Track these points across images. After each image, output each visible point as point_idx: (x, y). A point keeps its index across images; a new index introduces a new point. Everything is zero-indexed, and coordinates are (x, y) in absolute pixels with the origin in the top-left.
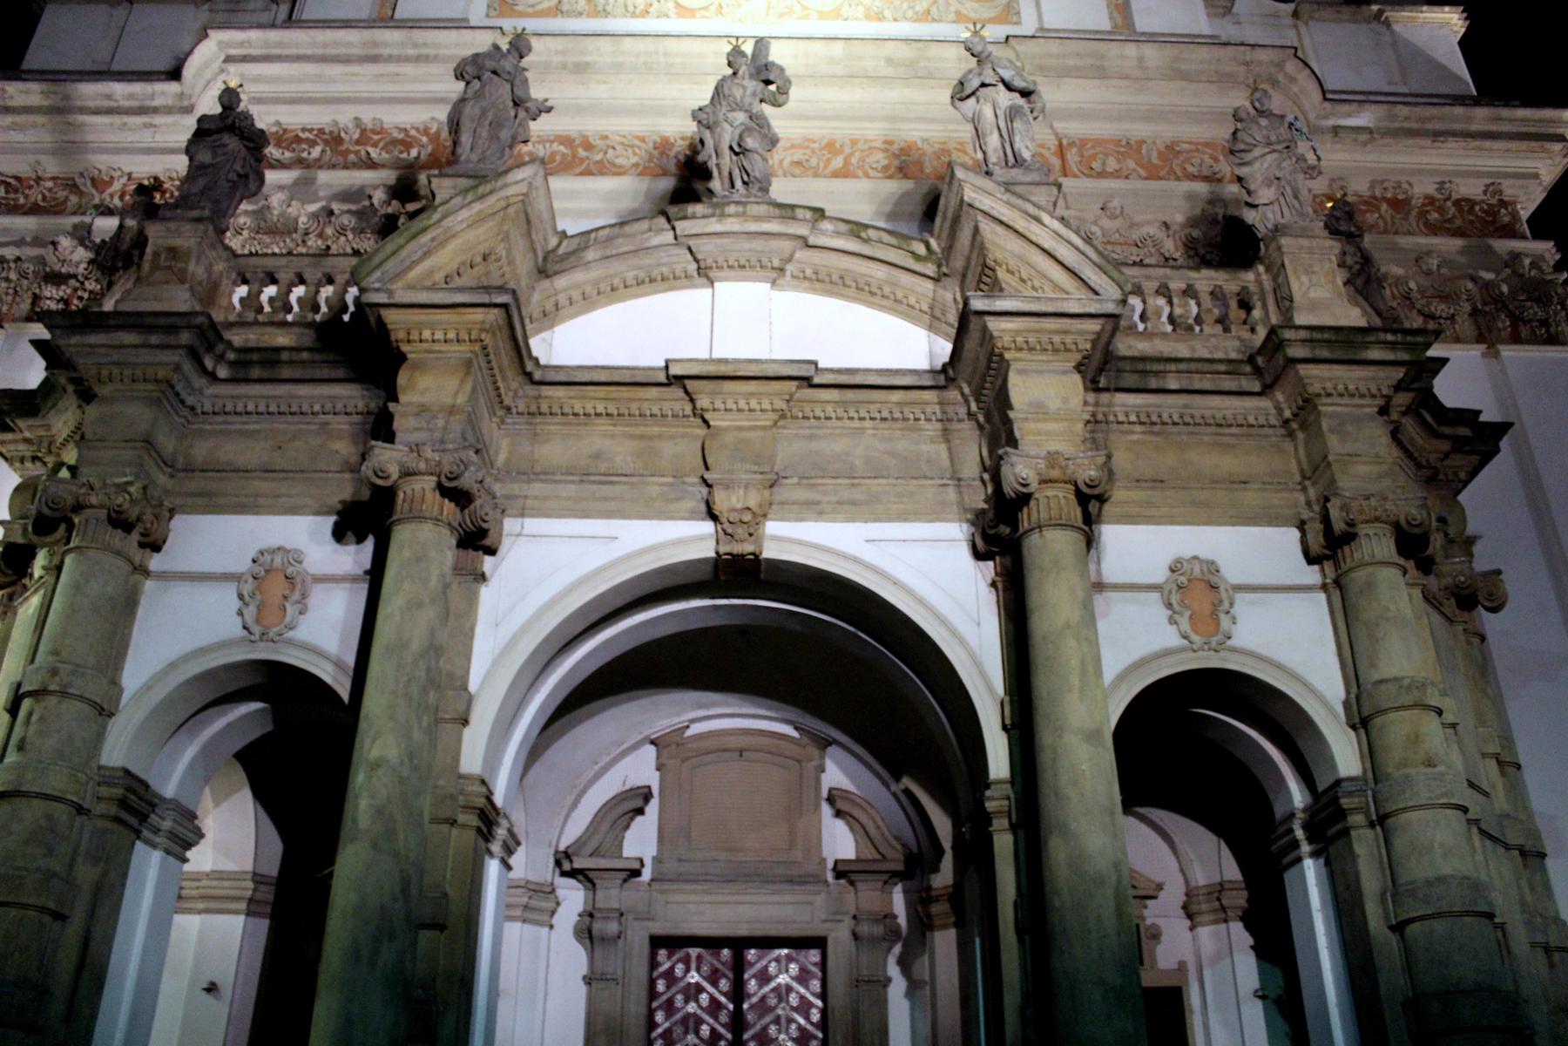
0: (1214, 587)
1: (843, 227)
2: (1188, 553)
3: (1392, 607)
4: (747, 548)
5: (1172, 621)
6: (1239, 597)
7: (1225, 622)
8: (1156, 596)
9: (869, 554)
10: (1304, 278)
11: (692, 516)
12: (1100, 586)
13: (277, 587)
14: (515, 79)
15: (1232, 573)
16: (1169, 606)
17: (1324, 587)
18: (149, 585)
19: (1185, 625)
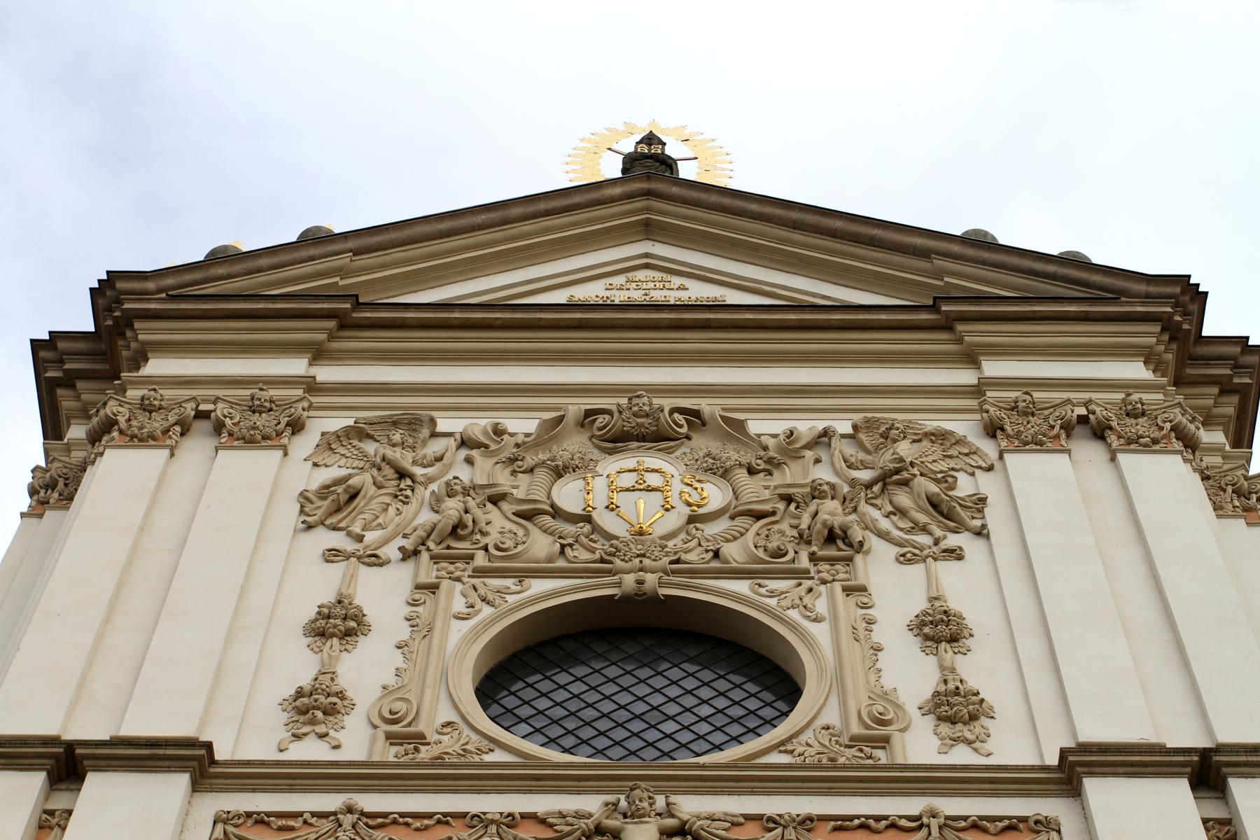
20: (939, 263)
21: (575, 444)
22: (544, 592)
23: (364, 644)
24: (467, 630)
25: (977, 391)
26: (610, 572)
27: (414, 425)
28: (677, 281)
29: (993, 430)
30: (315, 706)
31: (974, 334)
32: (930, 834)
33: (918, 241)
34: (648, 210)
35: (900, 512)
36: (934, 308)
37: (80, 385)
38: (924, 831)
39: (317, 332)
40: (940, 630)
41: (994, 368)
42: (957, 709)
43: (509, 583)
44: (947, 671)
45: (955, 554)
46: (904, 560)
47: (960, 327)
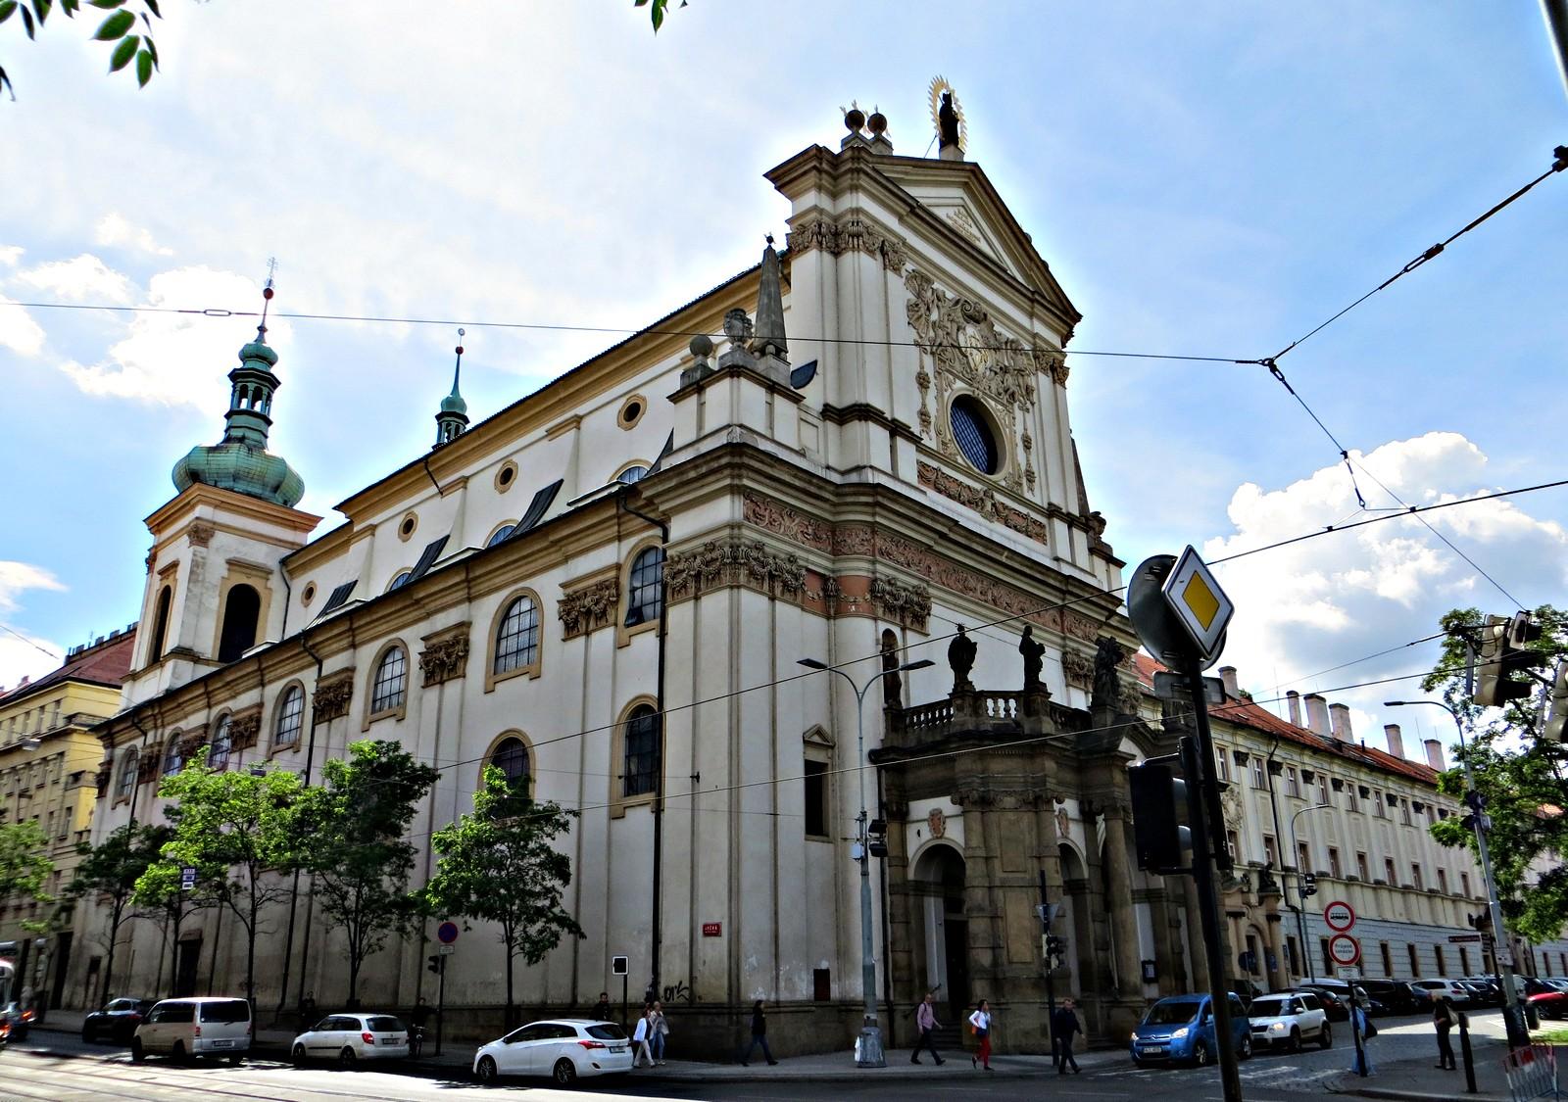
20: (1033, 265)
21: (958, 314)
22: (960, 387)
23: (929, 391)
24: (949, 396)
25: (1035, 335)
26: (971, 385)
27: (929, 281)
28: (970, 222)
29: (1036, 357)
30: (924, 415)
31: (1038, 309)
33: (1032, 254)
34: (969, 178)
35: (1019, 386)
36: (1033, 293)
37: (824, 176)
39: (903, 209)
40: (1027, 443)
41: (1039, 328)
42: (1030, 476)
43: (951, 377)
44: (1028, 464)
45: (1028, 410)
46: (1020, 408)
47: (1036, 305)
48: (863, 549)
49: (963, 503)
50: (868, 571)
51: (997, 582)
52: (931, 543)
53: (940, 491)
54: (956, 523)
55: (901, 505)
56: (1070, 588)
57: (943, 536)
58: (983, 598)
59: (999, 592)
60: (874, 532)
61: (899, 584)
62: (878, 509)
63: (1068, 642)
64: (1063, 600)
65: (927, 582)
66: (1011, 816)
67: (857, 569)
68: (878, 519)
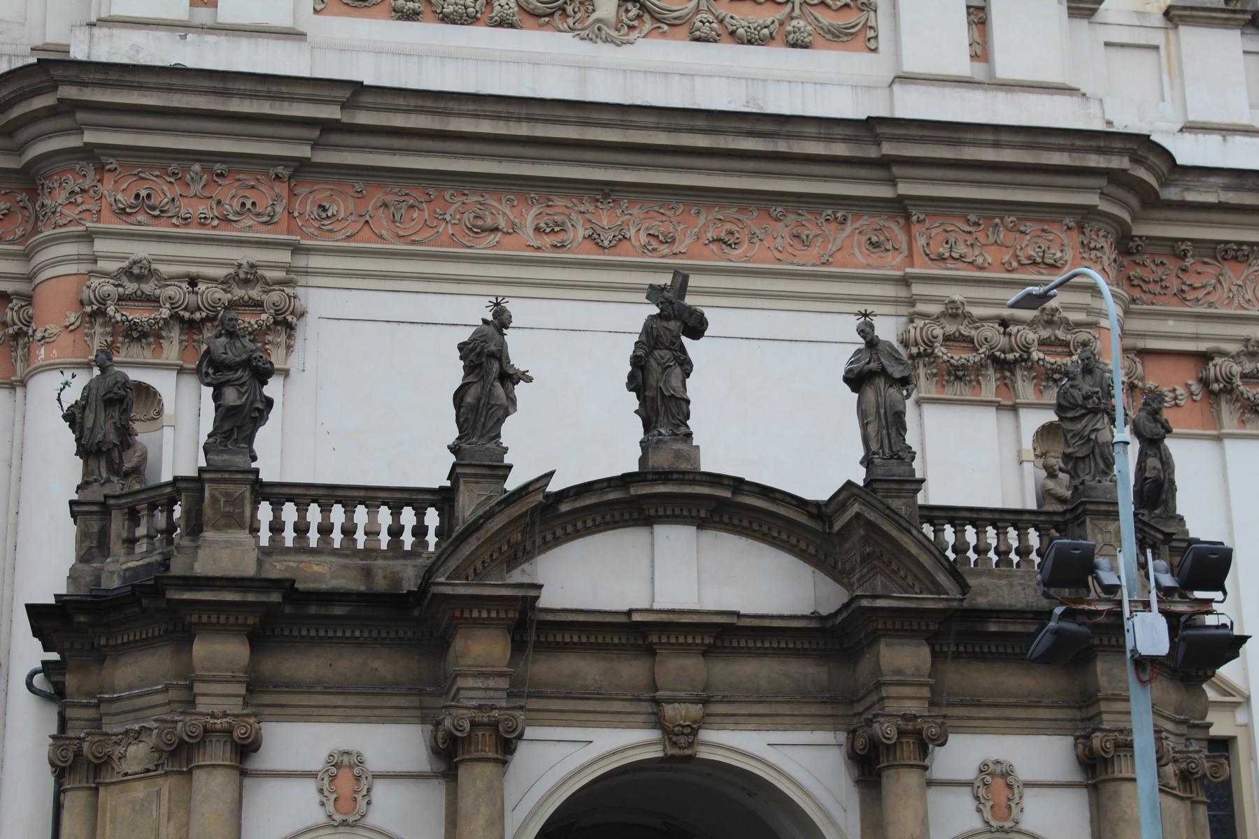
0: (1010, 786)
1: (756, 490)
2: (995, 757)
3: (1129, 812)
4: (687, 752)
5: (979, 811)
6: (1028, 792)
7: (1015, 810)
8: (968, 789)
9: (771, 755)
10: (1099, 537)
11: (645, 725)
12: (931, 783)
13: (345, 782)
14: (500, 355)
15: (1023, 772)
16: (977, 798)
17: (1087, 786)
18: (247, 781)
19: (988, 815)
32: (793, 9)
38: (790, 5)
48: (72, 212)
49: (503, 23)
50: (79, 259)
51: (606, 191)
52: (304, 151)
53: (412, 16)
54: (358, 87)
55: (140, 87)
56: (888, 149)
57: (328, 126)
58: (548, 240)
59: (606, 218)
60: (101, 169)
61: (164, 269)
62: (80, 116)
63: (917, 289)
64: (893, 182)
65: (296, 249)
66: (139, 791)
67: (60, 263)
68: (90, 137)
